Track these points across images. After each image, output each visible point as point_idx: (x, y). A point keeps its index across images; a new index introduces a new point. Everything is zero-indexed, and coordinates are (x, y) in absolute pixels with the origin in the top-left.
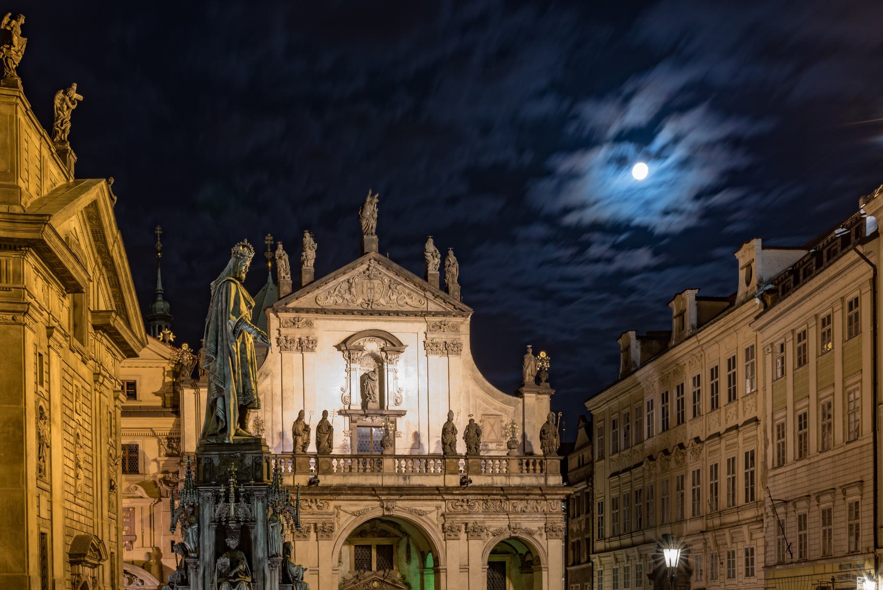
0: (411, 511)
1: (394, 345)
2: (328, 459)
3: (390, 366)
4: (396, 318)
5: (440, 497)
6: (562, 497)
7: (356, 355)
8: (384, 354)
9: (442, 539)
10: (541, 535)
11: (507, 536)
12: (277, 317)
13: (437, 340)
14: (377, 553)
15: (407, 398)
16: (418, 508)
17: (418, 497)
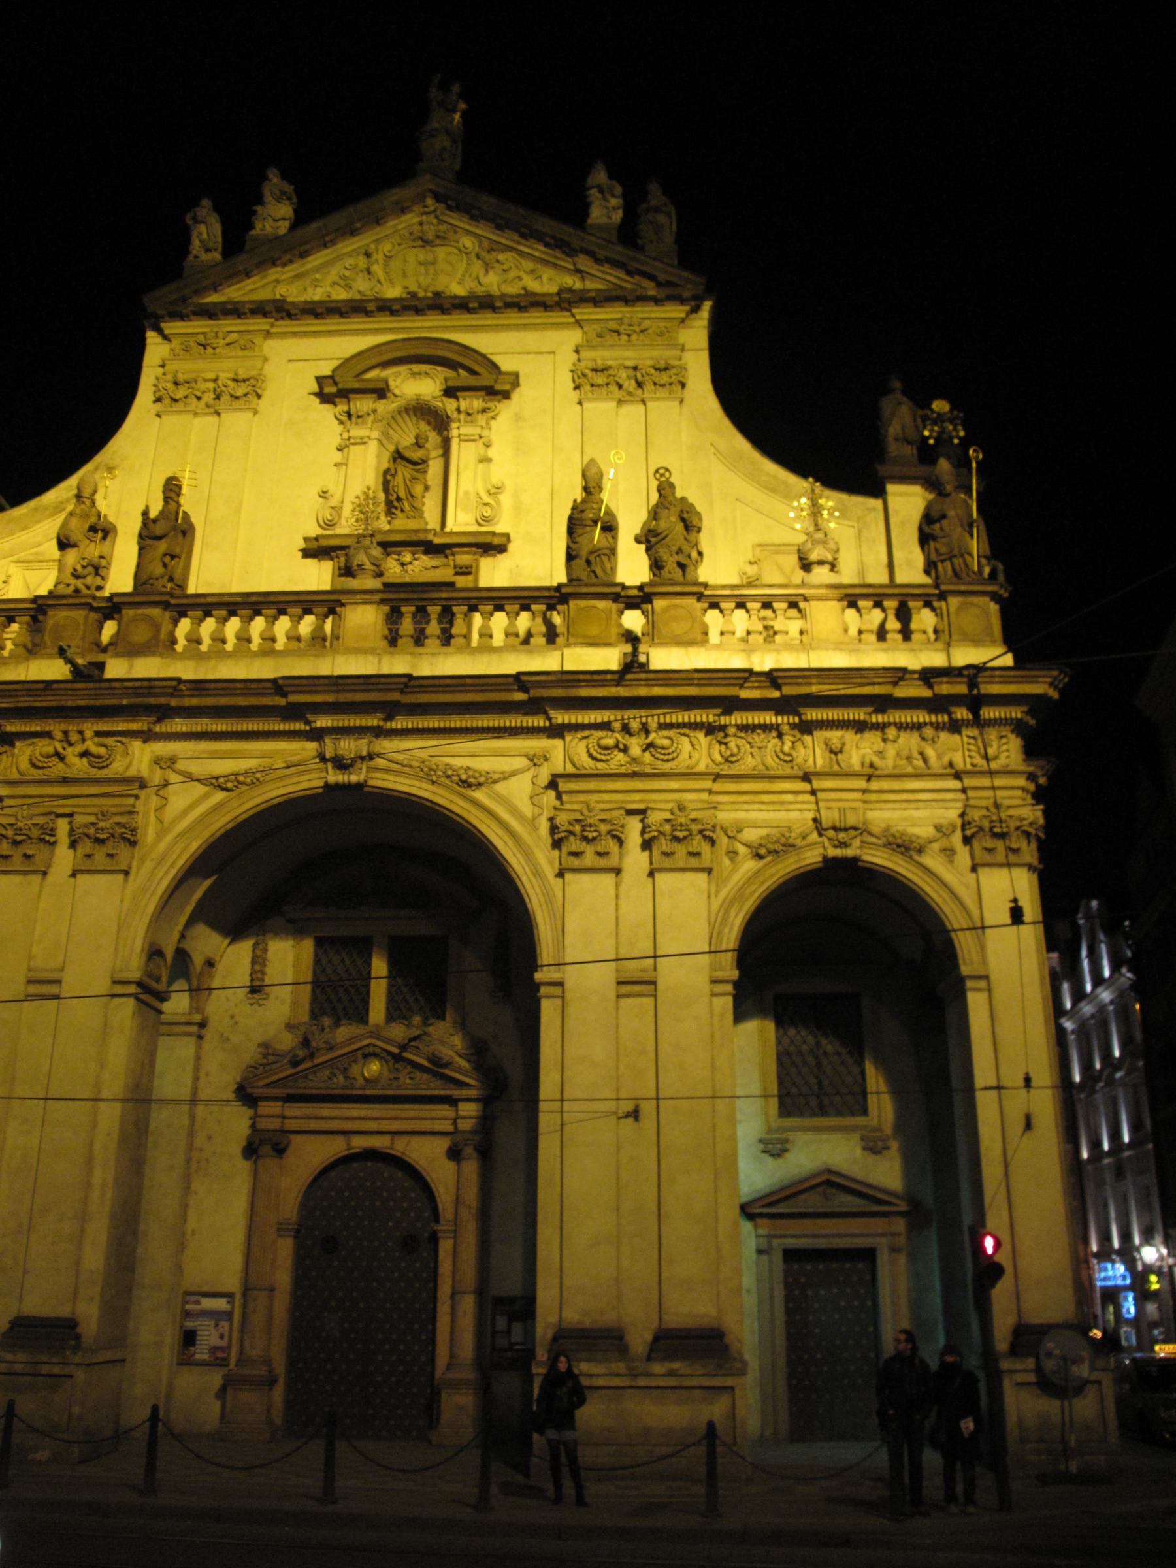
0: (429, 774)
1: (473, 372)
2: (155, 612)
3: (466, 430)
4: (488, 318)
5: (540, 721)
6: (1016, 712)
7: (362, 404)
8: (450, 405)
9: (549, 871)
10: (949, 852)
11: (812, 857)
12: (166, 338)
13: (610, 363)
14: (393, 964)
15: (518, 509)
16: (457, 762)
17: (456, 722)
